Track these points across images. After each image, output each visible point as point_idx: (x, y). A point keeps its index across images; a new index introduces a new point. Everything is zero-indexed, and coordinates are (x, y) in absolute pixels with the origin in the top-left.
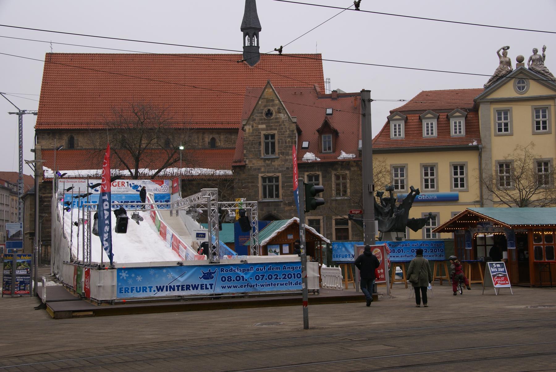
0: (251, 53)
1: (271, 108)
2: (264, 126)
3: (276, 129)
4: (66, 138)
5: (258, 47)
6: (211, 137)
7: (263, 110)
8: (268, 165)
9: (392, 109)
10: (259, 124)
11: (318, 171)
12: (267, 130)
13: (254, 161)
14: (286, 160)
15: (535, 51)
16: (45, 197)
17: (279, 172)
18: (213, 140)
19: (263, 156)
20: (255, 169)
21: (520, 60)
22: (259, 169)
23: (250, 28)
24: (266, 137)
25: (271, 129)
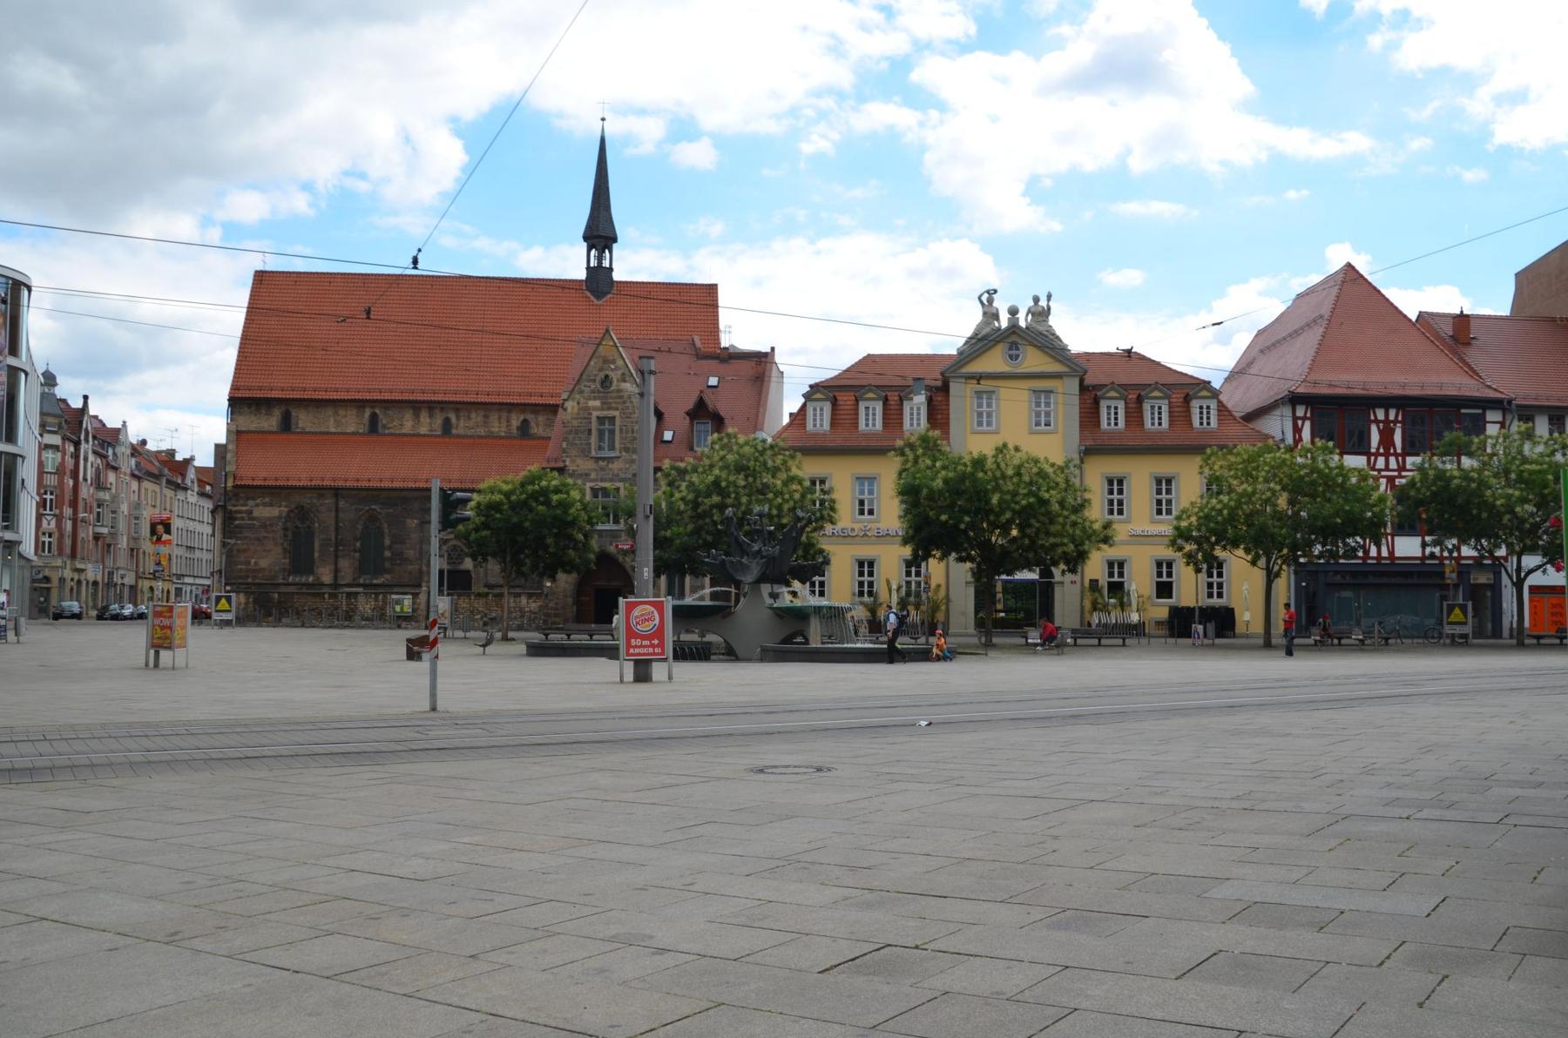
0: (599, 278)
1: (612, 374)
2: (597, 403)
4: (277, 413)
5: (611, 269)
8: (602, 469)
9: (812, 382)
10: (589, 398)
13: (579, 461)
14: (633, 461)
15: (1036, 300)
17: (622, 480)
18: (525, 421)
19: (593, 453)
20: (580, 476)
21: (1013, 312)
23: (599, 237)
24: (601, 420)
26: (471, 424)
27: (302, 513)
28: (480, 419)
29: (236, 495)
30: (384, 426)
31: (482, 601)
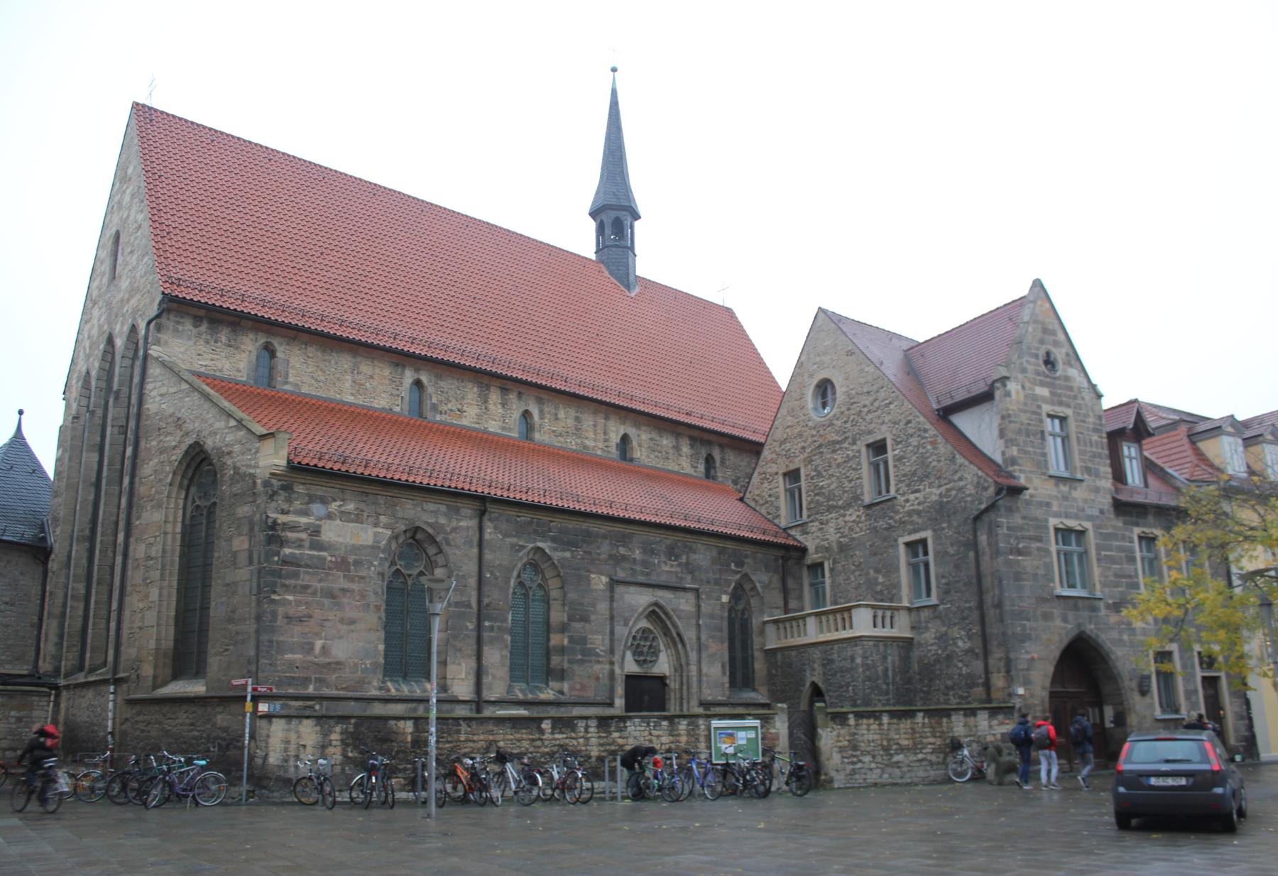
1: (1054, 350)
3: (1068, 406)
6: (622, 432)
7: (1038, 349)
8: (1065, 498)
11: (1155, 527)
12: (1053, 404)
16: (293, 528)
17: (1089, 518)
20: (1040, 504)
22: (1048, 505)
25: (1061, 404)
26: (558, 428)
27: (417, 542)
28: (570, 422)
29: (287, 488)
30: (434, 408)
31: (906, 725)
